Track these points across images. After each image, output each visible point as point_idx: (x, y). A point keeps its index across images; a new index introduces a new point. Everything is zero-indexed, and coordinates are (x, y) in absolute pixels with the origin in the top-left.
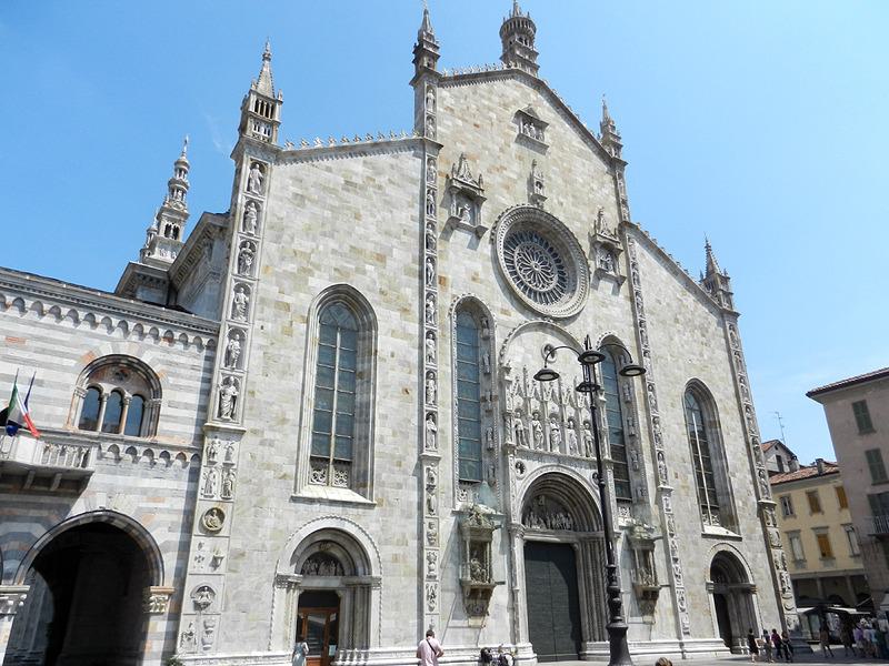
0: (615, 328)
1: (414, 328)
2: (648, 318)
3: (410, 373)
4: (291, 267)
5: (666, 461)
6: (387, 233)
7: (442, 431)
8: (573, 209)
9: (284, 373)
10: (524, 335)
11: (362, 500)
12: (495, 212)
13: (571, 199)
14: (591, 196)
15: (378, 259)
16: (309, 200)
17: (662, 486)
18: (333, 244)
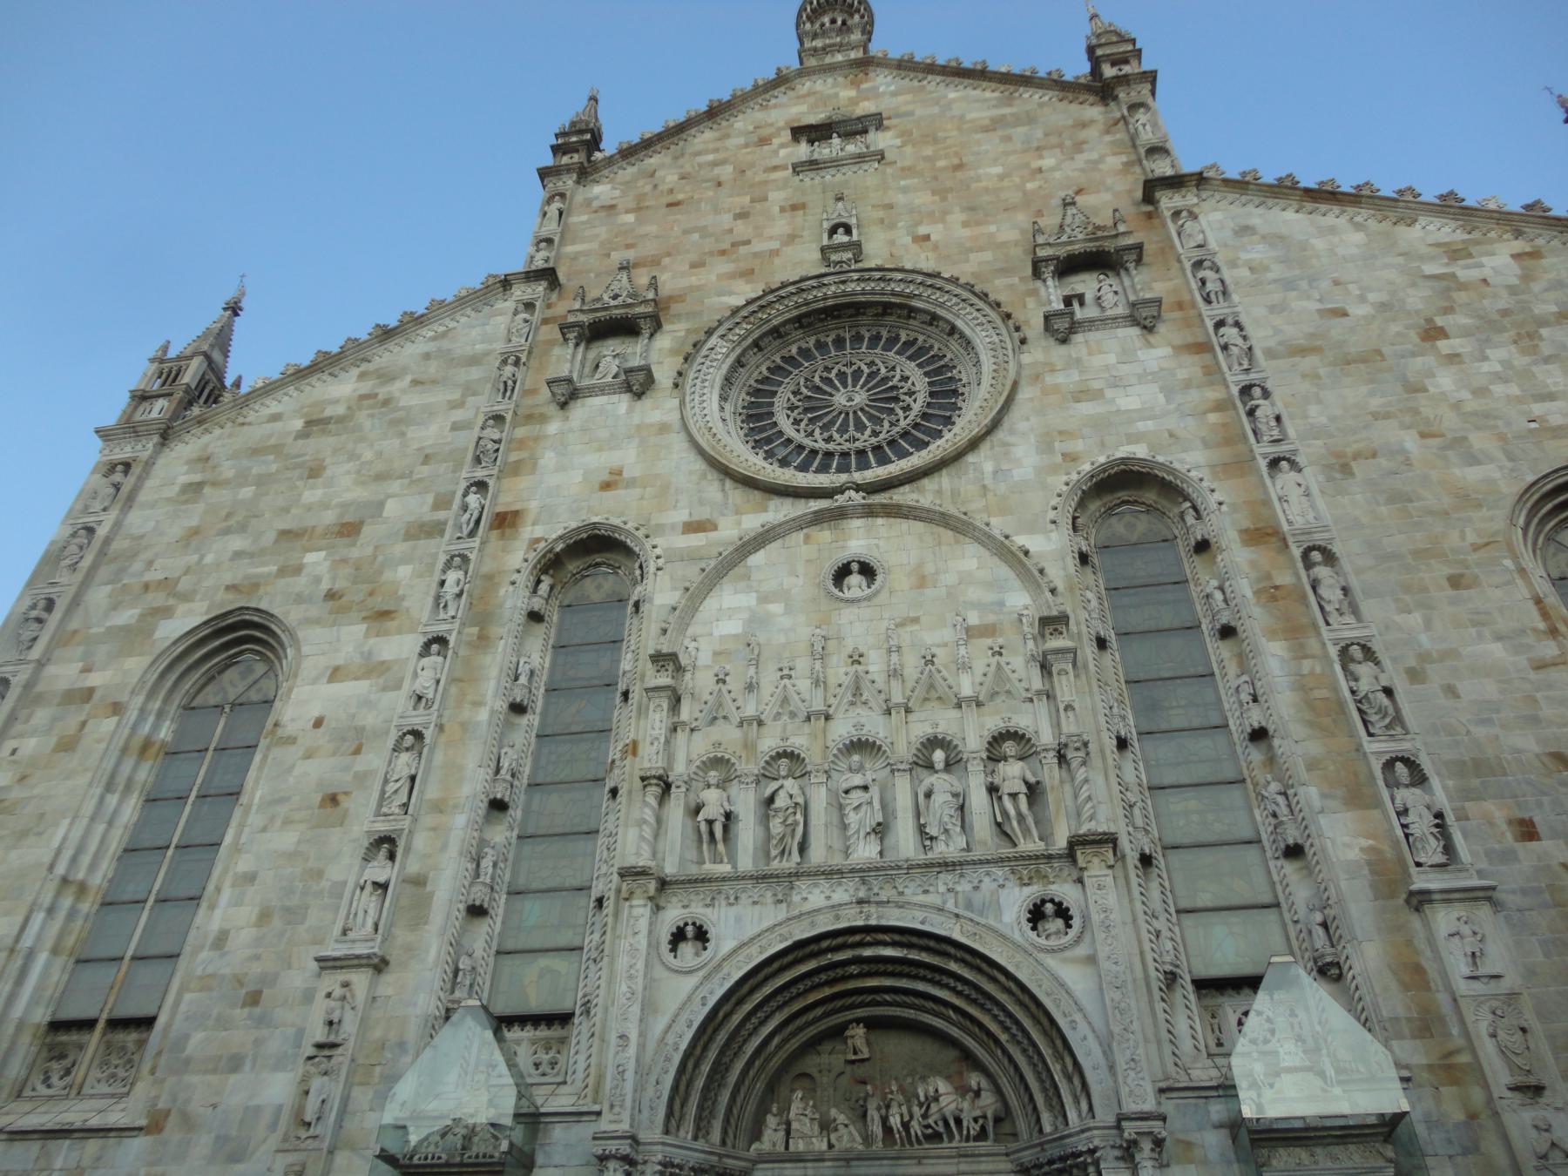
0: (1134, 438)
1: (401, 646)
2: (1269, 371)
3: (357, 751)
4: (127, 616)
5: (1435, 782)
6: (381, 477)
7: (419, 881)
8: (966, 233)
9: (23, 834)
10: (757, 559)
11: (115, 1118)
12: (696, 331)
13: (957, 217)
14: (1030, 186)
15: (340, 534)
16: (214, 484)
17: (1421, 881)
18: (237, 543)
